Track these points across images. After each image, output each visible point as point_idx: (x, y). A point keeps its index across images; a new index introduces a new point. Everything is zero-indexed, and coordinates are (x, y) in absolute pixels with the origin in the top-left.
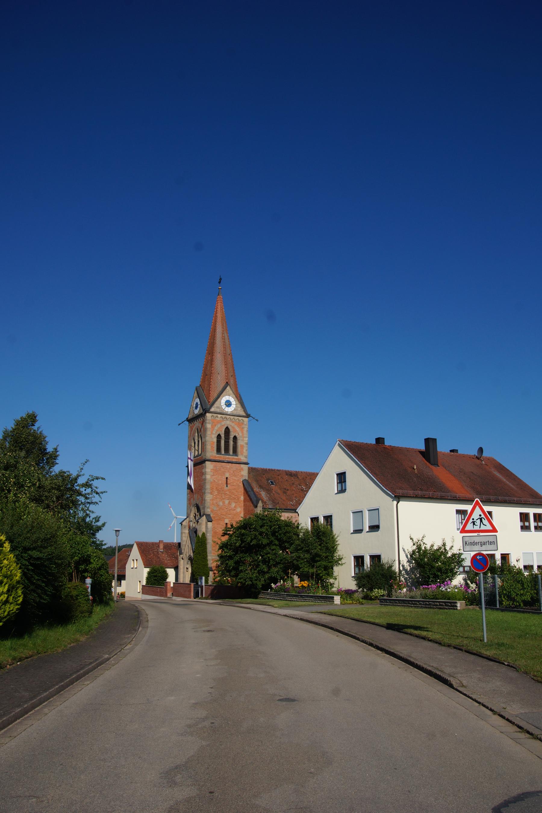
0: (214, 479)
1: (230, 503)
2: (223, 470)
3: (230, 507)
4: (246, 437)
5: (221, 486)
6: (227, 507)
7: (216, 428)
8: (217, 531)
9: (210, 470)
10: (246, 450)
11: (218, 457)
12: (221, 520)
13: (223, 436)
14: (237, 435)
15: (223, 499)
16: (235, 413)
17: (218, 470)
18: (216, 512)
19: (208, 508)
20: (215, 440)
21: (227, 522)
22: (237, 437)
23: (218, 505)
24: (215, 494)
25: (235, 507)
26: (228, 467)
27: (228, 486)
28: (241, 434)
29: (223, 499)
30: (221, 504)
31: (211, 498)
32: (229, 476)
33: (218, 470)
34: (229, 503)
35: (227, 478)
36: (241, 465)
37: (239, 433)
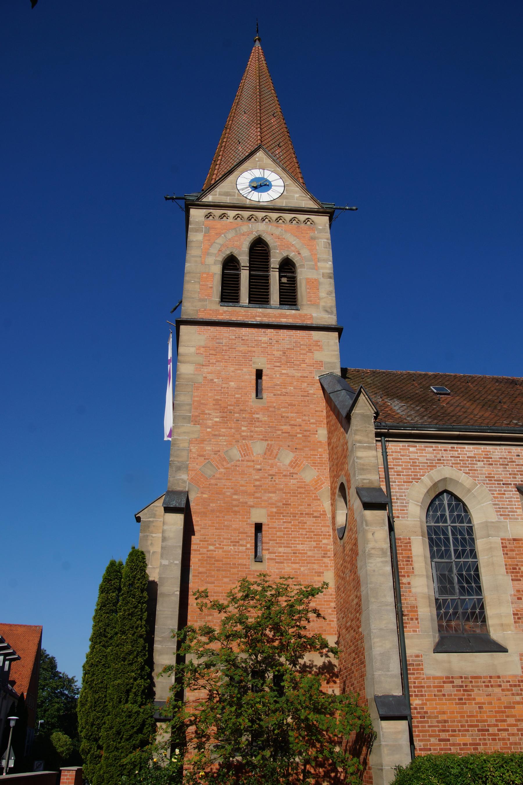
0: (210, 377)
1: (269, 452)
2: (243, 348)
3: (272, 466)
4: (326, 261)
5: (237, 396)
6: (259, 467)
7: (220, 240)
8: (219, 553)
9: (192, 350)
10: (329, 293)
11: (225, 312)
12: (236, 513)
13: (244, 259)
14: (292, 255)
15: (244, 438)
16: (283, 203)
17: (224, 348)
18: (213, 481)
19: (179, 469)
20: (217, 269)
21: (259, 521)
22: (296, 260)
23: (224, 459)
24: (209, 423)
25: (294, 464)
26: (265, 339)
27: (265, 395)
28: (305, 253)
29: (244, 438)
30: (235, 453)
31: (196, 436)
32: (269, 366)
33: (224, 348)
34: (269, 449)
35: (259, 374)
36: (314, 333)
37: (301, 252)
